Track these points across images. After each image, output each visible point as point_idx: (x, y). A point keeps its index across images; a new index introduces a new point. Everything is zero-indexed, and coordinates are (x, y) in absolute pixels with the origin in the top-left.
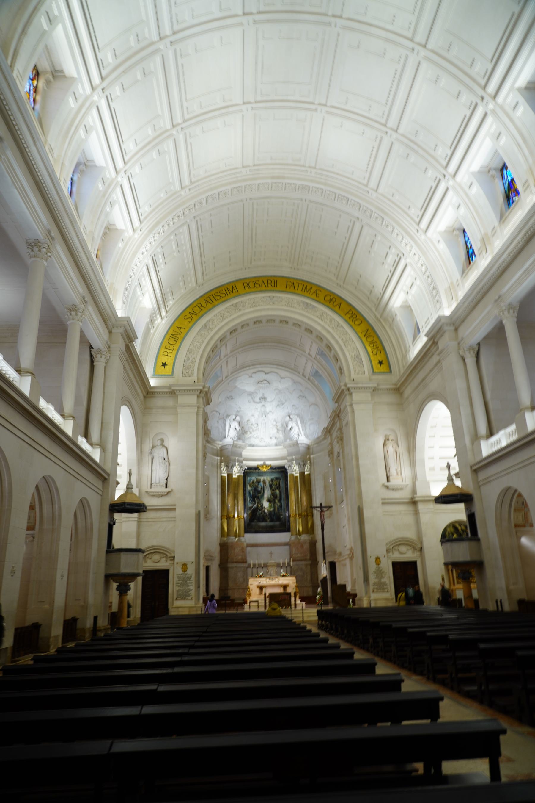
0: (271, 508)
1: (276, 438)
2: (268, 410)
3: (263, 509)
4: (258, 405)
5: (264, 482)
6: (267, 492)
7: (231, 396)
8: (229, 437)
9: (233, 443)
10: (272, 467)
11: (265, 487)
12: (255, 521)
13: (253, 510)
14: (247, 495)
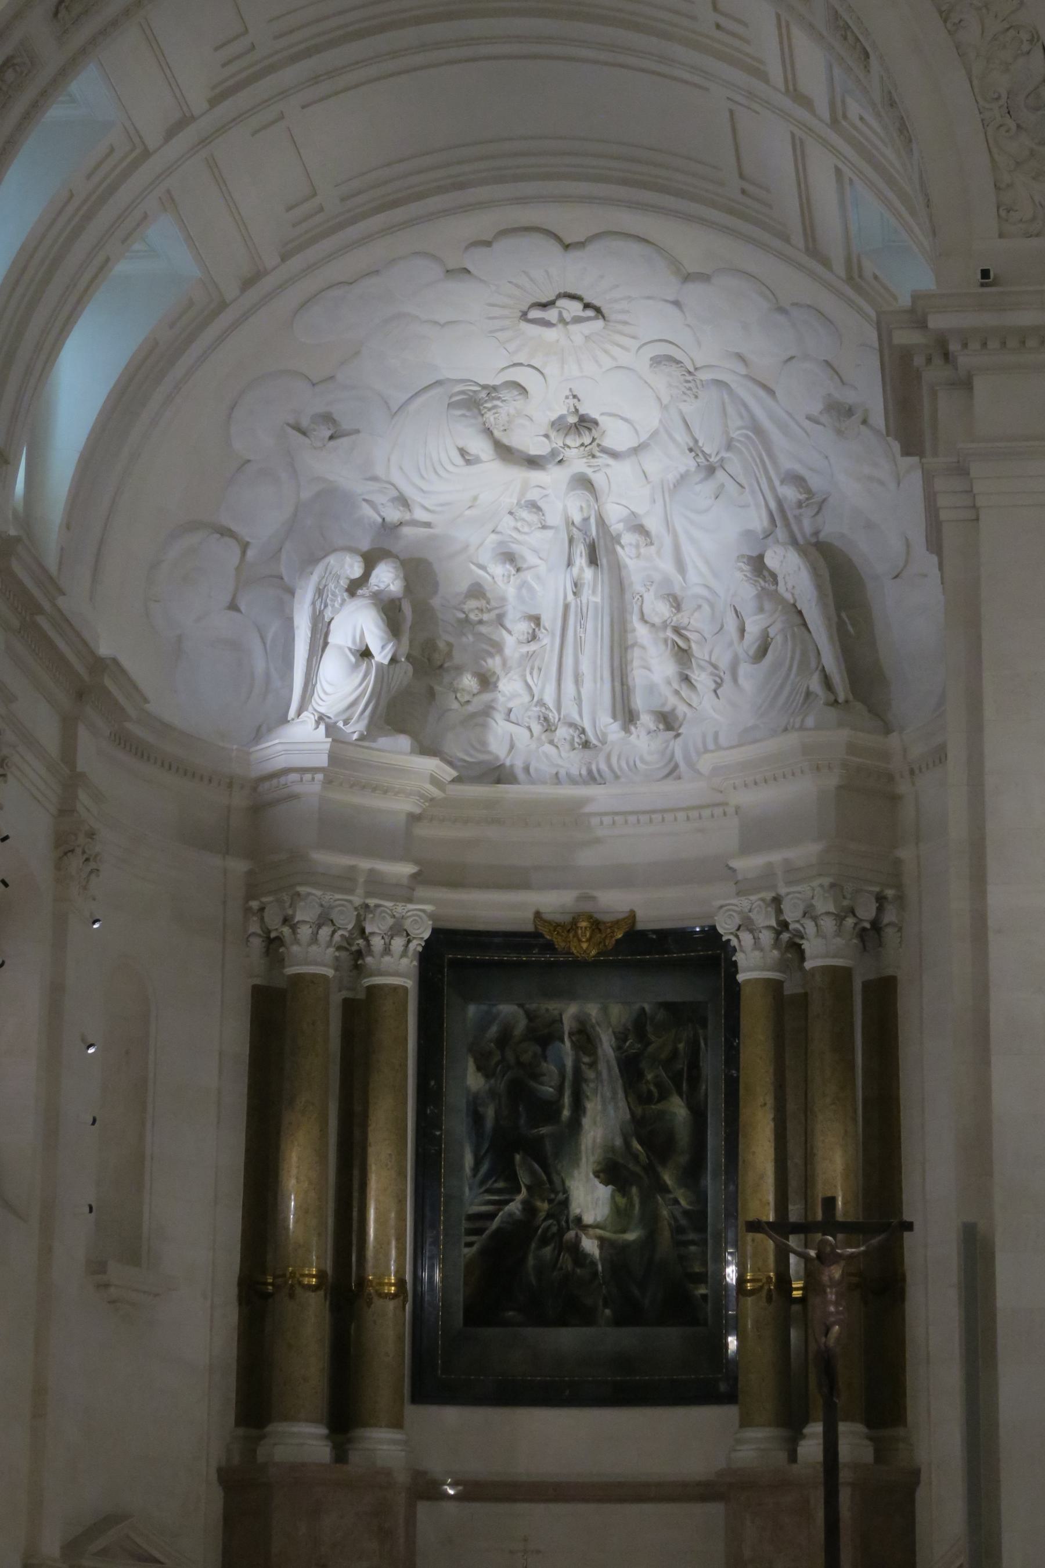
0: (624, 1231)
2: (615, 514)
3: (571, 1234)
4: (536, 476)
6: (604, 1110)
7: (328, 418)
8: (309, 718)
9: (333, 757)
10: (643, 933)
11: (590, 1074)
12: (511, 1313)
13: (498, 1231)
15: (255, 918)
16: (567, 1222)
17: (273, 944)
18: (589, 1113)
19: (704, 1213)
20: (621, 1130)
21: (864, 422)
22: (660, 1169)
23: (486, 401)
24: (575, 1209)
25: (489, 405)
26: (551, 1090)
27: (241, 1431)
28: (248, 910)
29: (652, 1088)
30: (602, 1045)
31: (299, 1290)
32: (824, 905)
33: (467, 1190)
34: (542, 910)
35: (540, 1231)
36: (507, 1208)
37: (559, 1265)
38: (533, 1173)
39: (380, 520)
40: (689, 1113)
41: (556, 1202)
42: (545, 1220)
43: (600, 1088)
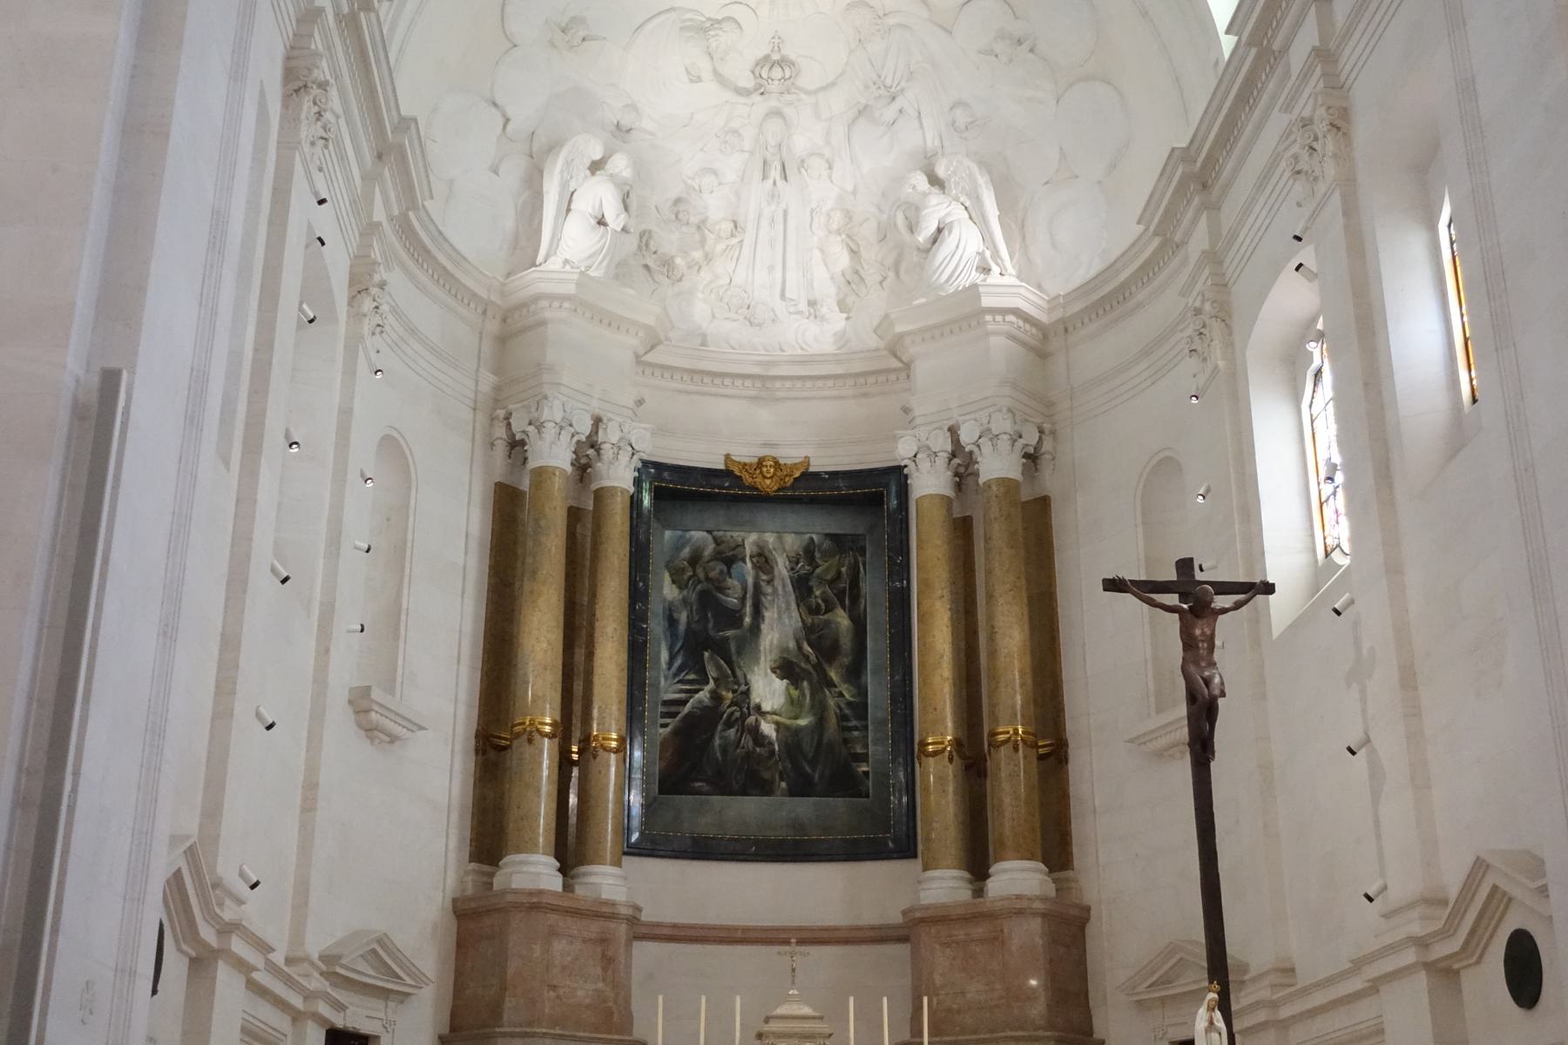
0: (796, 718)
1: (842, 306)
2: (800, 143)
3: (752, 719)
5: (763, 561)
6: (780, 617)
9: (579, 284)
10: (817, 475)
11: (769, 590)
12: (700, 784)
13: (687, 715)
14: (656, 626)
15: (501, 424)
16: (748, 708)
17: (516, 446)
18: (767, 621)
19: (865, 705)
20: (795, 638)
21: (1031, 50)
22: (826, 667)
23: (710, 30)
24: (755, 698)
25: (712, 33)
26: (735, 601)
27: (473, 866)
28: (493, 419)
29: (820, 601)
30: (777, 566)
31: (537, 736)
32: (1003, 424)
33: (662, 680)
34: (731, 453)
35: (725, 715)
36: (697, 696)
37: (741, 745)
38: (719, 668)
39: (616, 123)
40: (850, 622)
41: (739, 692)
42: (729, 707)
43: (776, 600)
